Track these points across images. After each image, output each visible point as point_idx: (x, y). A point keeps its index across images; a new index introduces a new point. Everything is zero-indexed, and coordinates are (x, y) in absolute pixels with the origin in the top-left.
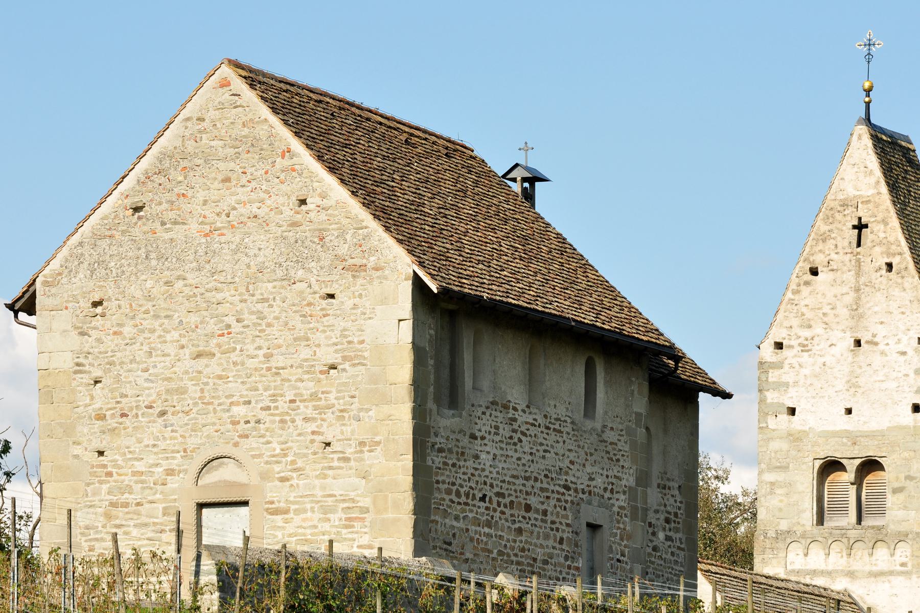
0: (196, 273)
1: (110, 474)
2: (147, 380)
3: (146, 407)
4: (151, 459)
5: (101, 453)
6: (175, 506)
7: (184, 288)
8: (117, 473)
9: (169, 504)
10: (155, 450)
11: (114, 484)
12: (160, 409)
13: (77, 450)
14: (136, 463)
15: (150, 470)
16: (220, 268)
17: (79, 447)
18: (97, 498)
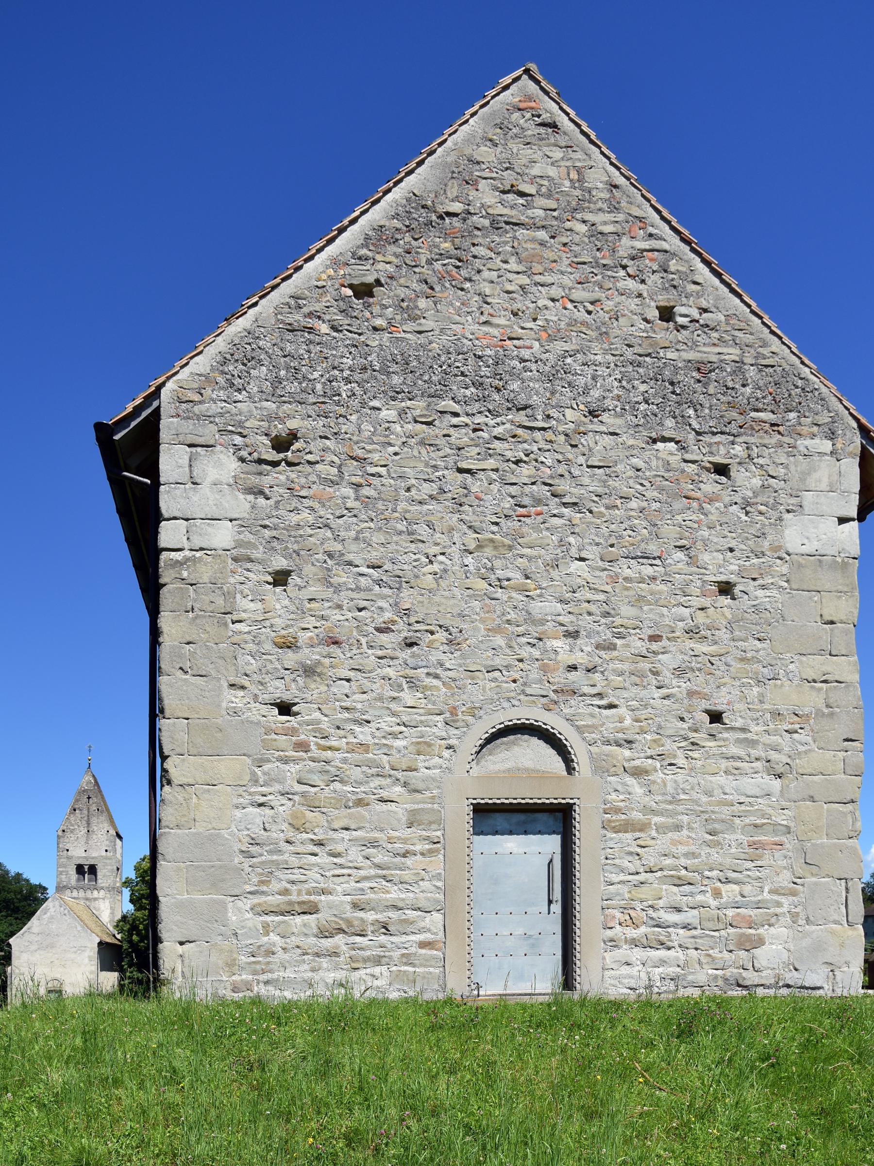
0: (477, 405)
1: (303, 746)
2: (379, 583)
3: (379, 630)
4: (387, 723)
5: (285, 709)
6: (433, 810)
7: (452, 431)
8: (317, 744)
9: (421, 806)
10: (393, 706)
11: (311, 763)
12: (405, 634)
13: (237, 699)
14: (357, 729)
15: (384, 741)
16: (522, 399)
17: (241, 693)
18: (277, 787)
